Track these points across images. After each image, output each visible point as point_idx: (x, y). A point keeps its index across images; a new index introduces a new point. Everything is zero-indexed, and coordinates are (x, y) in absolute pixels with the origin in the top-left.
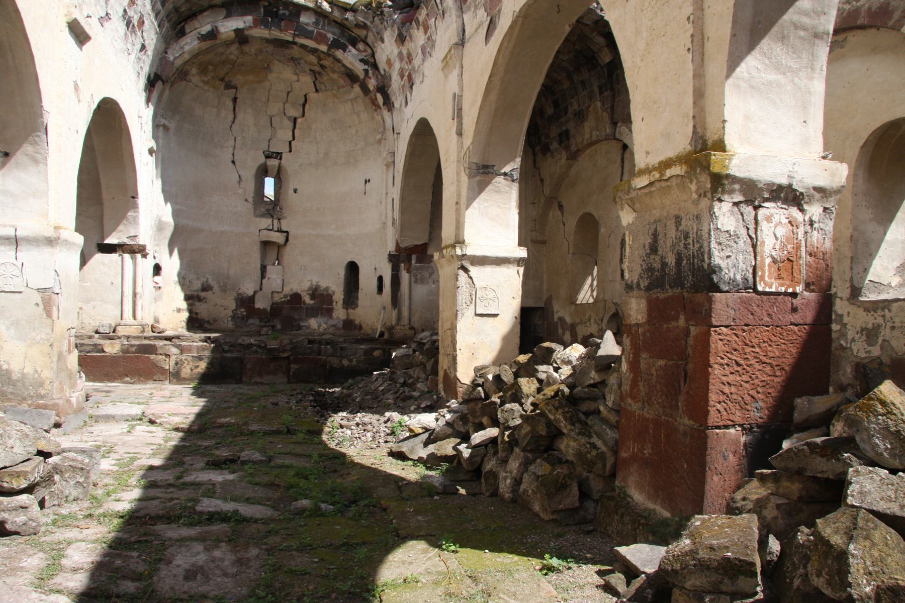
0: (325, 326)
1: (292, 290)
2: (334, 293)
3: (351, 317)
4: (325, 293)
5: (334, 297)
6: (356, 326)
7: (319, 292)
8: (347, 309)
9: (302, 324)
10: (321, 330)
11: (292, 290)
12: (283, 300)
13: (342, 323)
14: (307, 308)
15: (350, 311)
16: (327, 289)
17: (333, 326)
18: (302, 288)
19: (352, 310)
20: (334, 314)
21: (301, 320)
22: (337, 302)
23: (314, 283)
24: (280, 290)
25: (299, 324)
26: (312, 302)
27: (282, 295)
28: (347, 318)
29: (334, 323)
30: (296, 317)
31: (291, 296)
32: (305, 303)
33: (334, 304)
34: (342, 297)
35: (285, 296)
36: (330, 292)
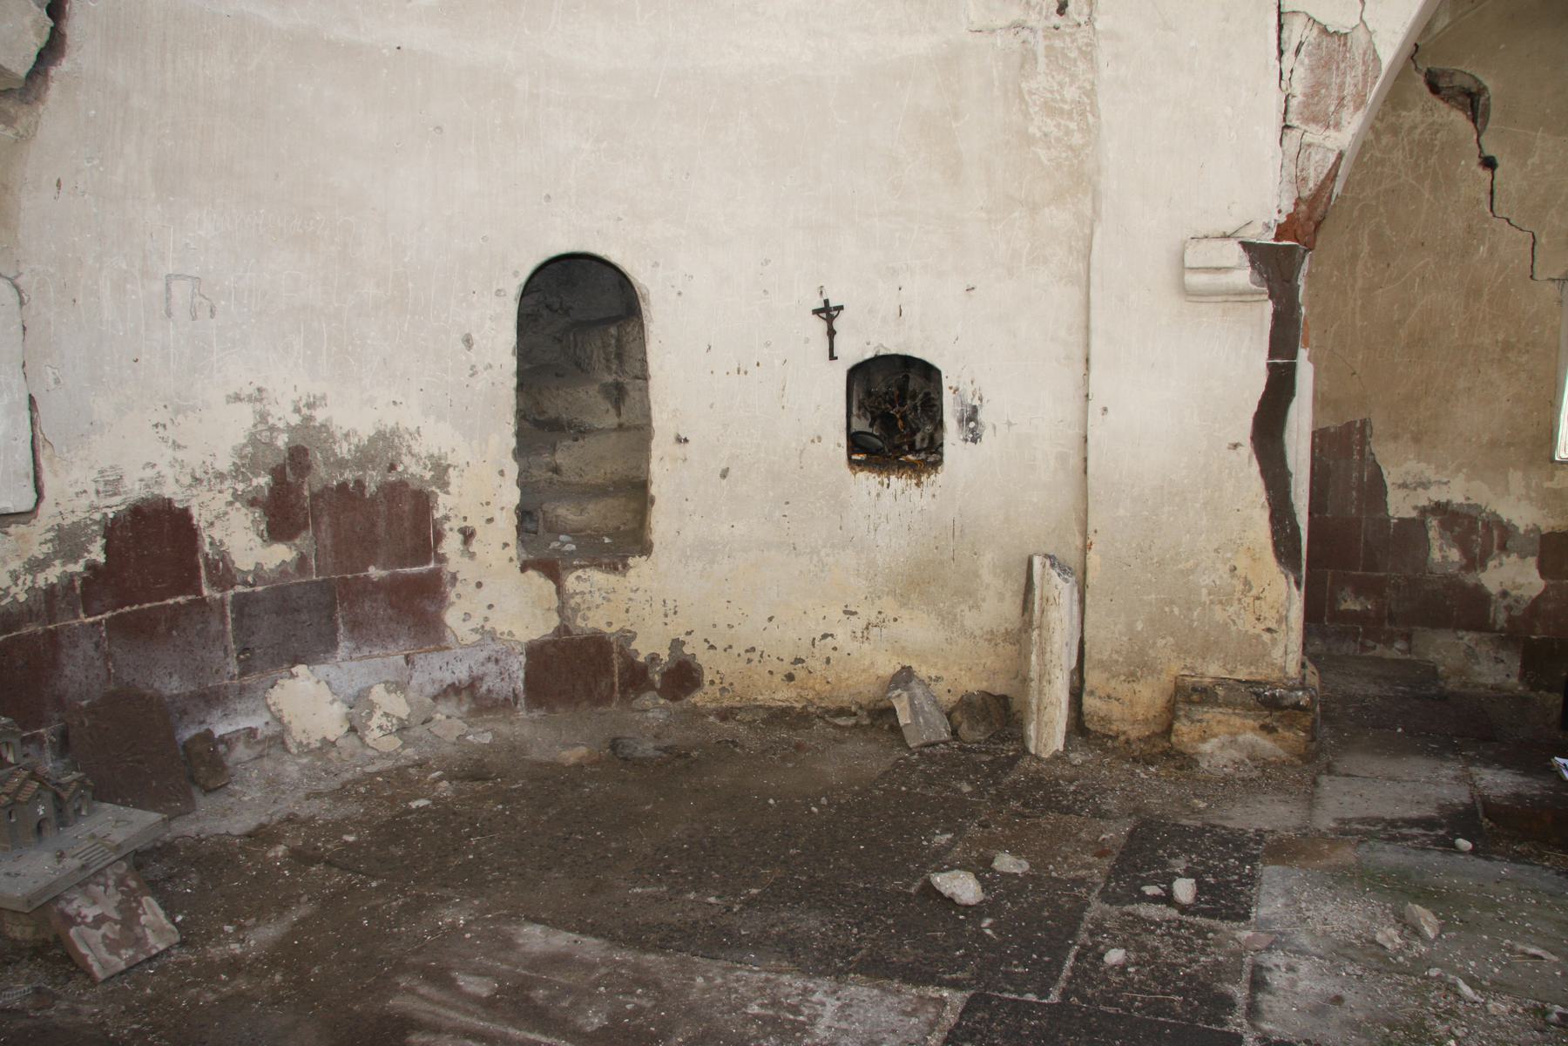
0: (398, 706)
1: (113, 485)
2: (441, 471)
3: (596, 620)
4: (373, 480)
5: (444, 504)
6: (636, 676)
7: (322, 475)
8: (551, 569)
9: (221, 729)
10: (377, 735)
11: (113, 485)
12: (53, 574)
13: (517, 666)
14: (241, 603)
15: (587, 582)
16: (383, 447)
17: (453, 691)
18: (194, 458)
19: (598, 577)
20: (452, 617)
21: (212, 699)
22: (468, 535)
23: (284, 415)
24: (26, 503)
25: (209, 733)
26: (280, 554)
27: (35, 539)
28: (563, 629)
29: (461, 673)
30: (173, 686)
31: (112, 530)
32: (223, 573)
33: (451, 545)
34: (513, 496)
35: (68, 541)
36: (413, 469)
